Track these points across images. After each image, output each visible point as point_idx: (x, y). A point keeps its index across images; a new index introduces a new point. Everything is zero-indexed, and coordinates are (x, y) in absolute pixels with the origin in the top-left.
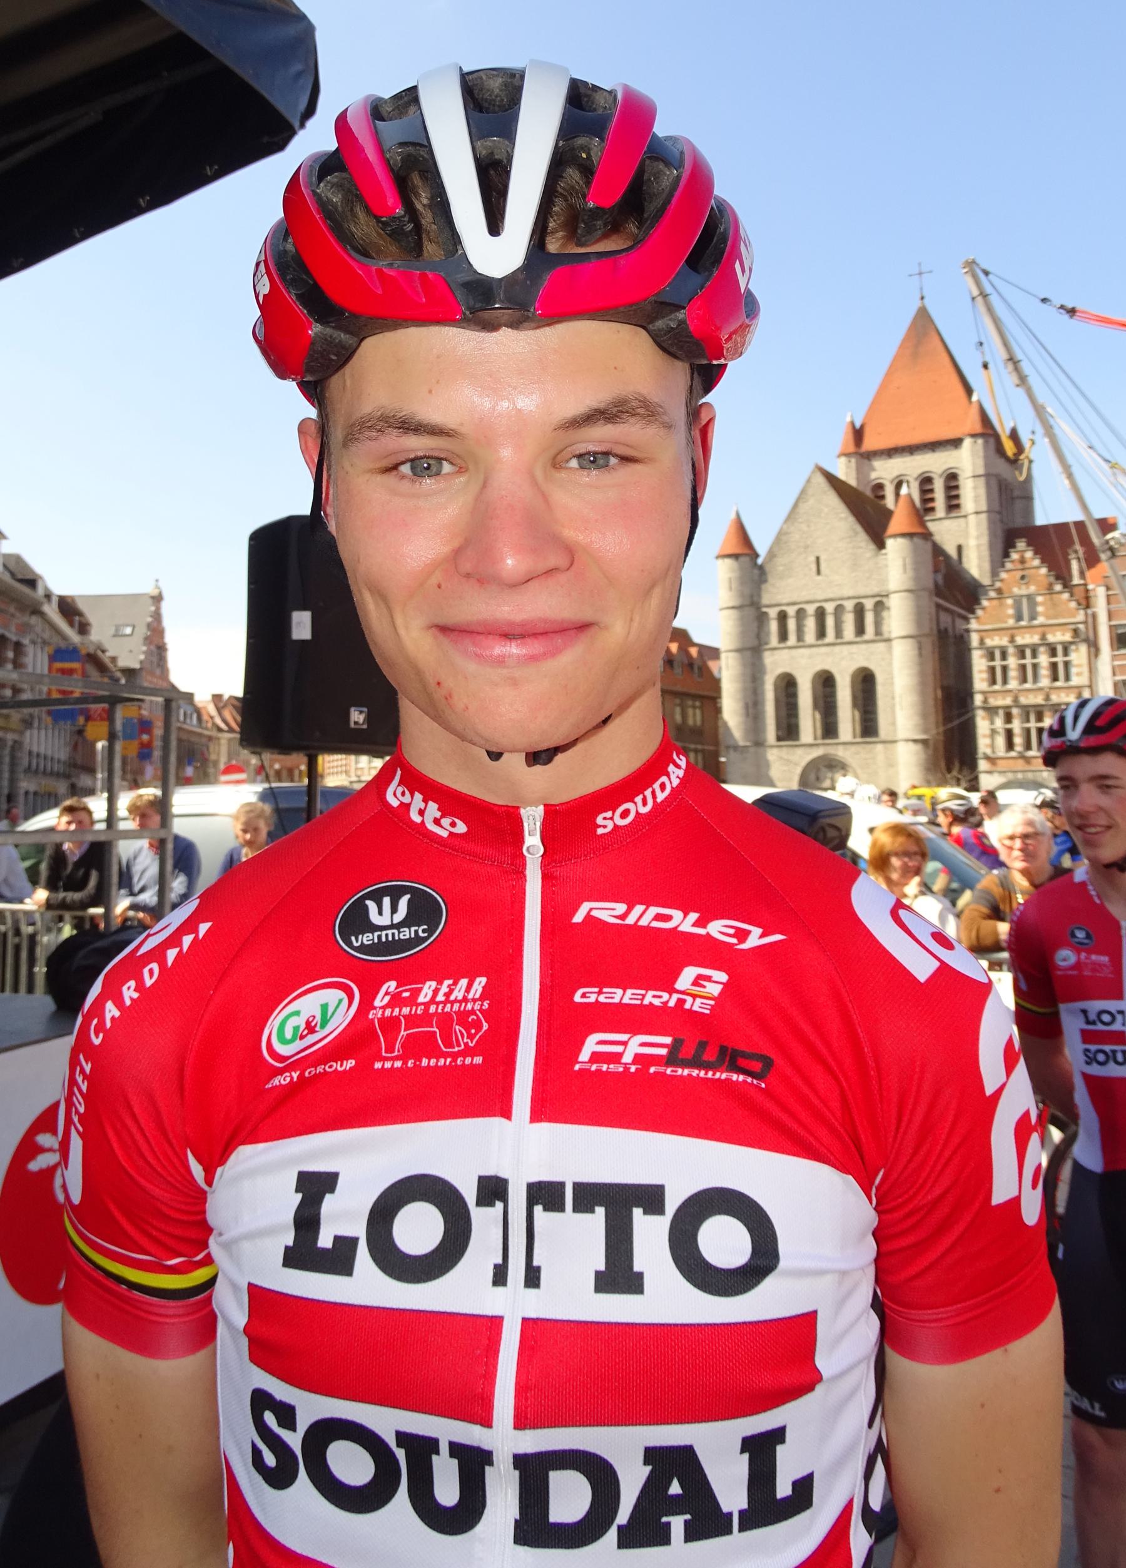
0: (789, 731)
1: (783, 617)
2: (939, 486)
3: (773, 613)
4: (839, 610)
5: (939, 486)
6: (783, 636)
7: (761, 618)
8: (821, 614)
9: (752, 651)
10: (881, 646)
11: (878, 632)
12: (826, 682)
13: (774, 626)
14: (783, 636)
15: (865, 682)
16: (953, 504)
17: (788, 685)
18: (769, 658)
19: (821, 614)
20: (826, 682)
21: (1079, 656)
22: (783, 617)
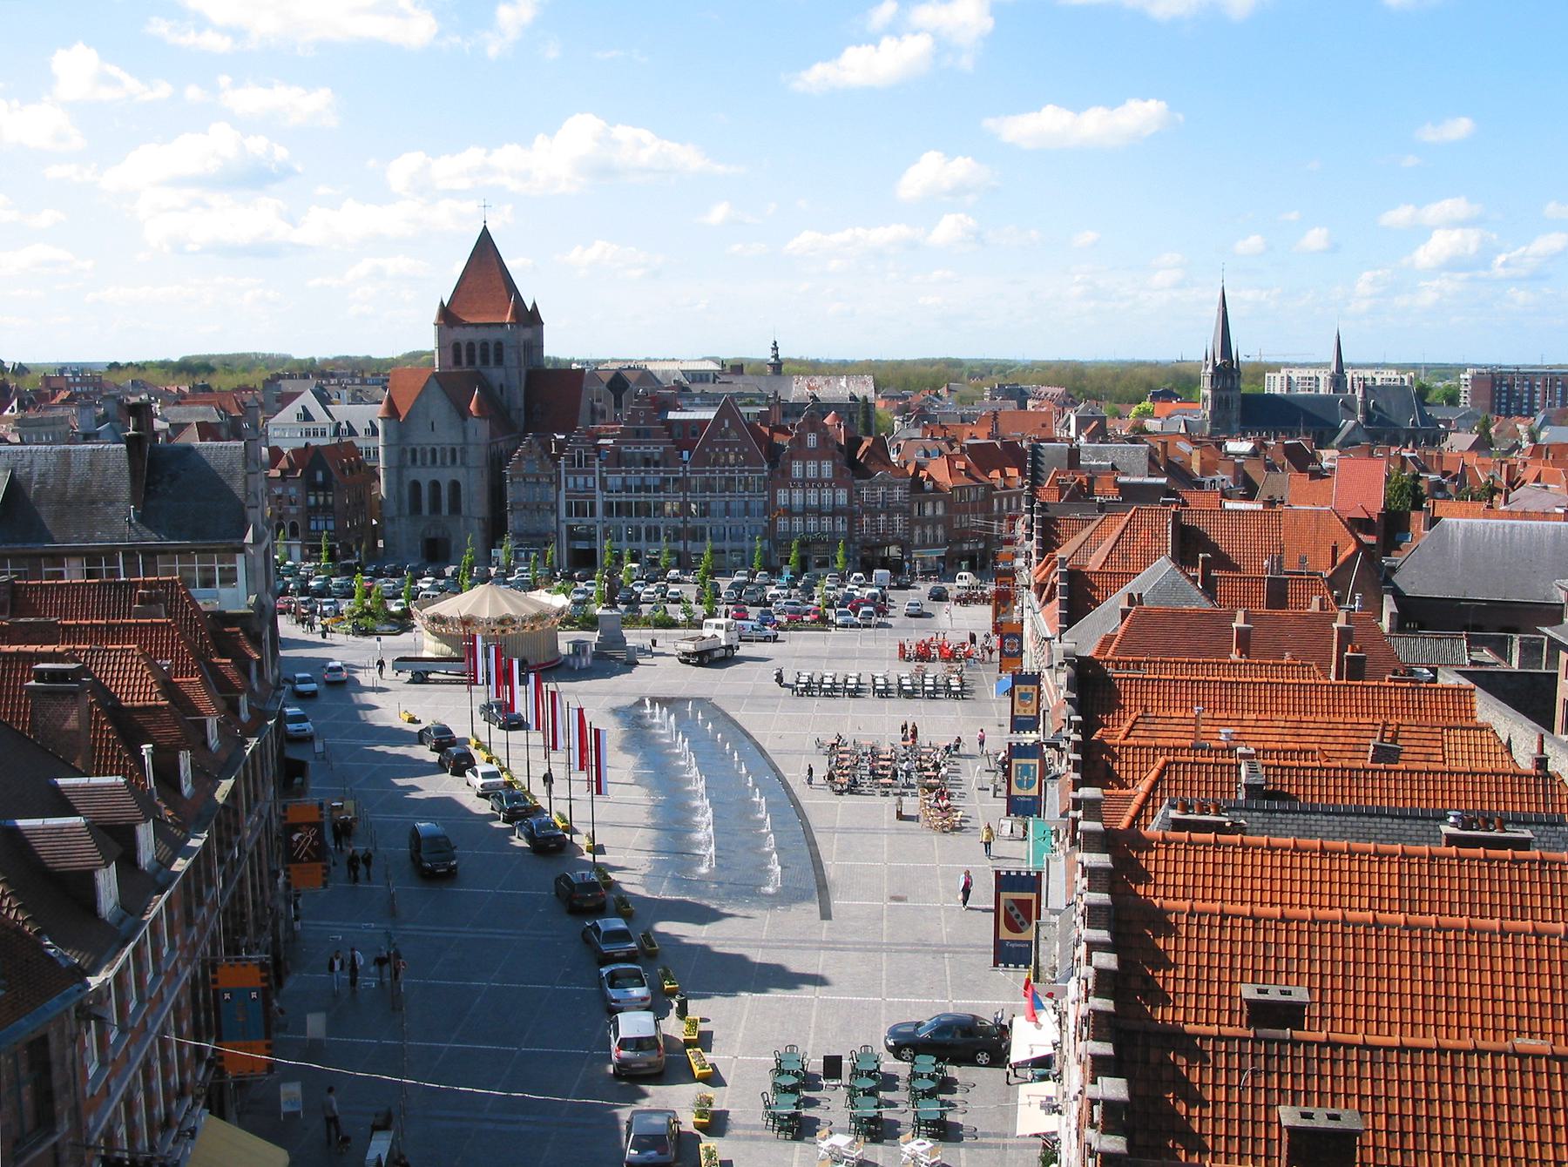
0: (416, 508)
1: (414, 451)
2: (491, 348)
3: (409, 449)
4: (443, 449)
5: (491, 348)
6: (414, 460)
7: (404, 451)
8: (434, 451)
9: (397, 469)
10: (463, 470)
11: (463, 463)
12: (435, 485)
13: (409, 456)
14: (414, 460)
15: (455, 485)
16: (499, 360)
17: (416, 485)
18: (406, 473)
19: (434, 451)
20: (435, 485)
21: (553, 489)
22: (414, 451)
